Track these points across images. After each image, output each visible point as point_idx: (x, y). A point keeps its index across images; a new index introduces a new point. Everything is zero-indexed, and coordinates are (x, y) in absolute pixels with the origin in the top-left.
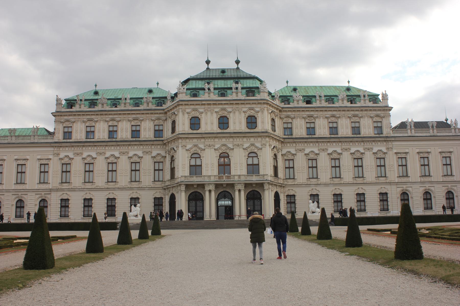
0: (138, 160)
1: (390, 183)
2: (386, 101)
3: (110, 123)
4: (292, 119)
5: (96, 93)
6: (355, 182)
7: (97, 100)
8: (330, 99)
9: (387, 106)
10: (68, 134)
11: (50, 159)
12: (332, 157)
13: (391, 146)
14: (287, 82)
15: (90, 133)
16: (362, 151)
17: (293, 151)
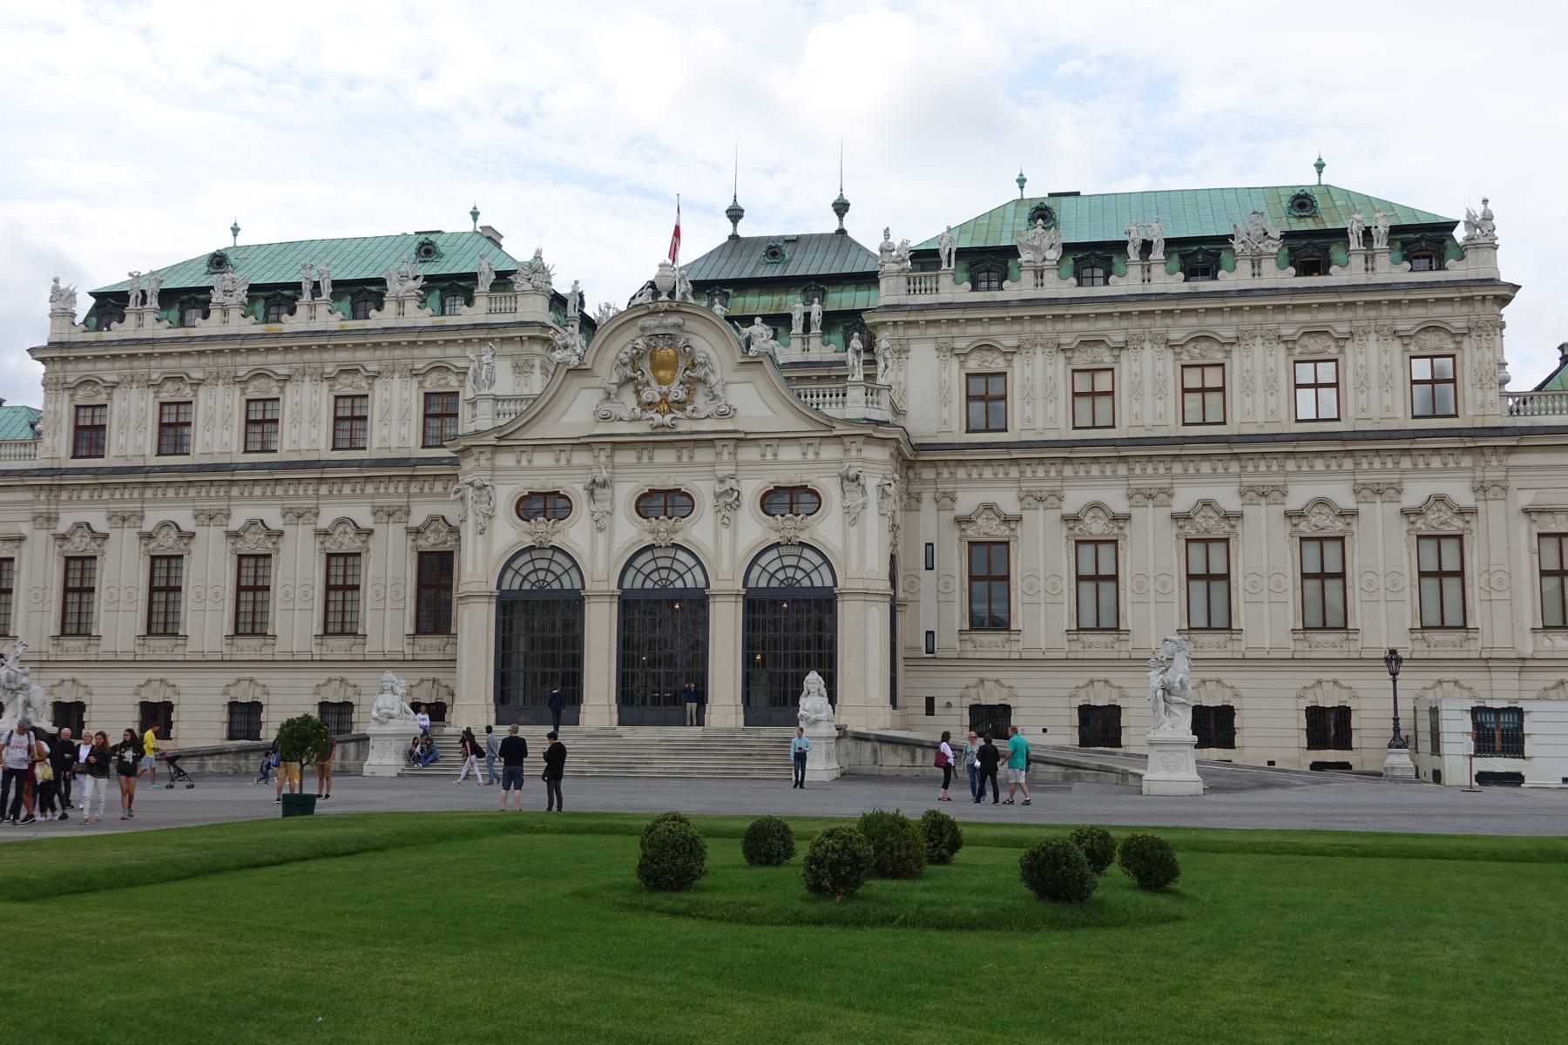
1: (1487, 663)
2: (1484, 254)
3: (253, 391)
4: (1010, 354)
5: (218, 261)
6: (1302, 649)
7: (207, 290)
8: (1199, 255)
9: (1492, 282)
10: (89, 436)
11: (21, 539)
12: (1193, 534)
13: (1494, 474)
14: (1021, 182)
15: (173, 432)
16: (1346, 501)
17: (1008, 502)
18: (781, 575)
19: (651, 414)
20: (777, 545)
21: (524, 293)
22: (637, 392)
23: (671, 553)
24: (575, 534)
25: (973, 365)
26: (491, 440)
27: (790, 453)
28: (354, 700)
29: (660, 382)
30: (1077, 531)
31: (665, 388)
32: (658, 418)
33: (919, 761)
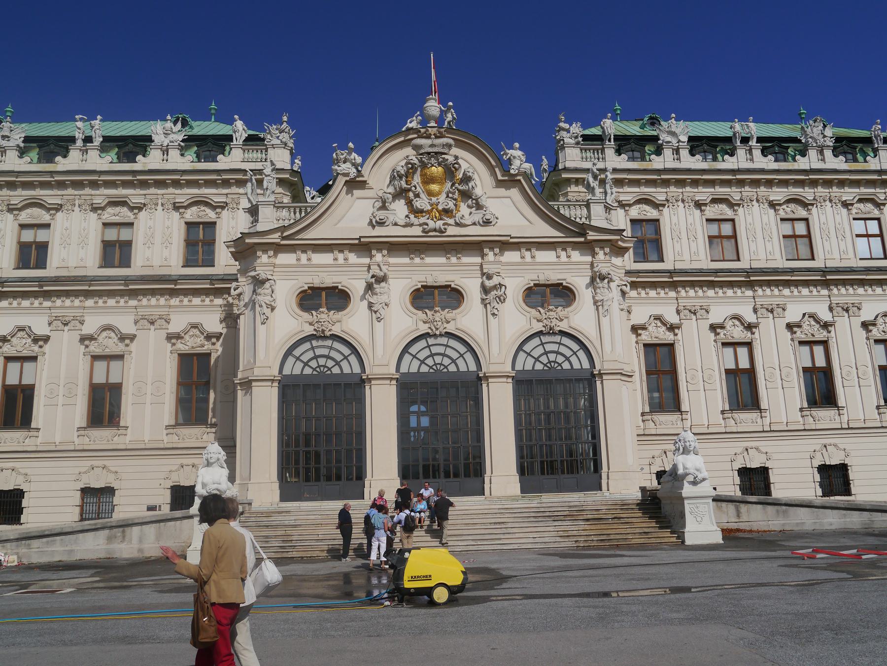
0: (119, 348)
12: (803, 338)
18: (544, 359)
19: (423, 220)
20: (539, 333)
21: (273, 146)
22: (409, 203)
23: (444, 340)
24: (353, 322)
25: (635, 212)
26: (275, 238)
27: (546, 256)
28: (115, 485)
29: (430, 194)
30: (722, 335)
31: (434, 199)
32: (430, 222)
33: (744, 517)
